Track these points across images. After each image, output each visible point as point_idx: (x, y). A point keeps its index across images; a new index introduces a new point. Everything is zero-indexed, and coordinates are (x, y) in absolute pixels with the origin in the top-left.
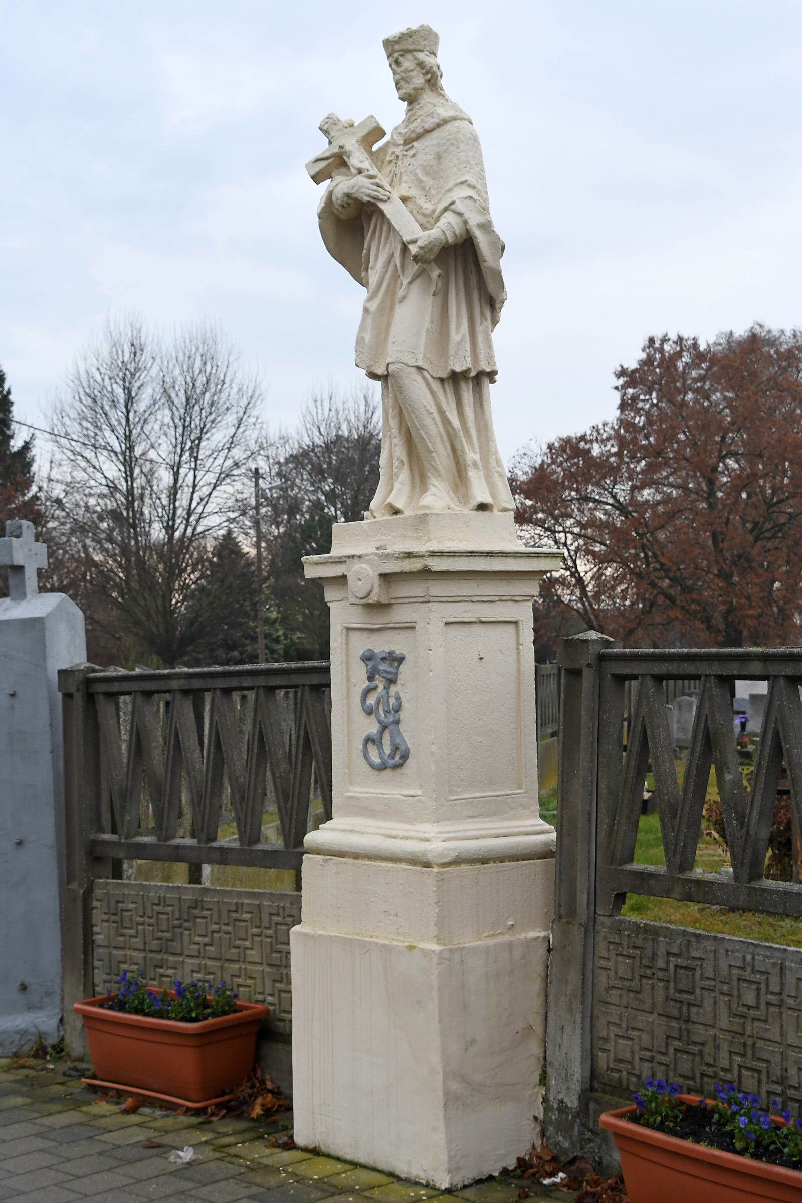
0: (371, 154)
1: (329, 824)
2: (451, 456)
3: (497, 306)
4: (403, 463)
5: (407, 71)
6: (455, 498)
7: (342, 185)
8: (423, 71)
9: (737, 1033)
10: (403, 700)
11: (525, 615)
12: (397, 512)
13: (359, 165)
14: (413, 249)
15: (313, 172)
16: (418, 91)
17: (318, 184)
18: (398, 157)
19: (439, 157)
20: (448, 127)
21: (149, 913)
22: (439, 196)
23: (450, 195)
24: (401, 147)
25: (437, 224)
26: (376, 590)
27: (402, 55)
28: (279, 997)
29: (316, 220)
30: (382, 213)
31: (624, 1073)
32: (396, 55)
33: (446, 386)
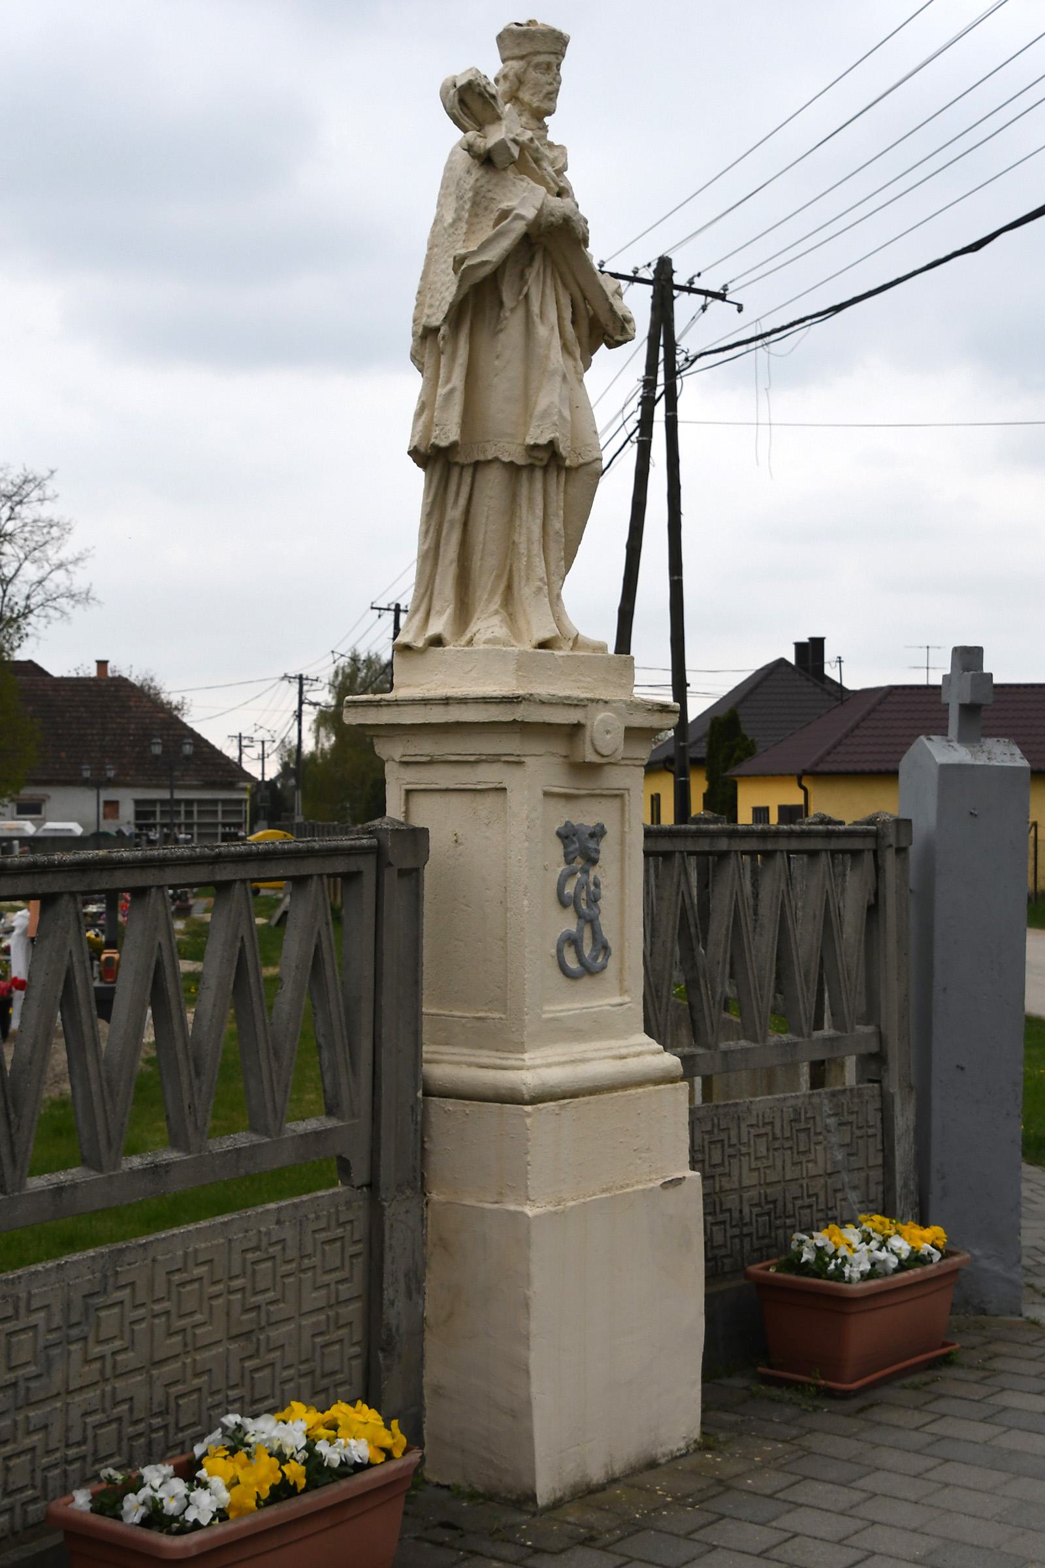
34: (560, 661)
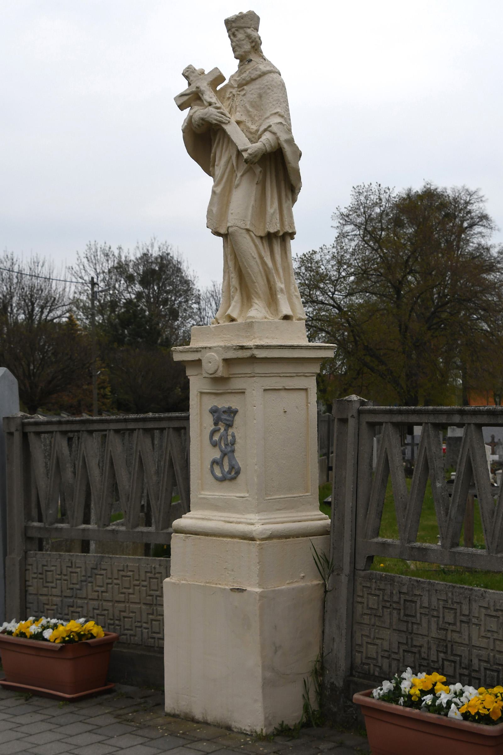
0: (216, 92)
1: (188, 515)
2: (267, 285)
3: (297, 191)
4: (237, 289)
5: (240, 40)
6: (269, 312)
7: (199, 112)
8: (250, 41)
9: (441, 639)
10: (237, 437)
11: (312, 384)
12: (233, 320)
13: (209, 100)
14: (245, 155)
15: (179, 103)
16: (247, 53)
17: (182, 110)
18: (234, 95)
19: (260, 96)
20: (266, 77)
21: (64, 572)
22: (261, 121)
23: (267, 121)
24: (236, 89)
25: (260, 140)
26: (221, 369)
27: (237, 30)
28: (151, 623)
29: (181, 134)
30: (224, 132)
31: (372, 665)
32: (233, 30)
33: (264, 242)
34: (213, 329)
